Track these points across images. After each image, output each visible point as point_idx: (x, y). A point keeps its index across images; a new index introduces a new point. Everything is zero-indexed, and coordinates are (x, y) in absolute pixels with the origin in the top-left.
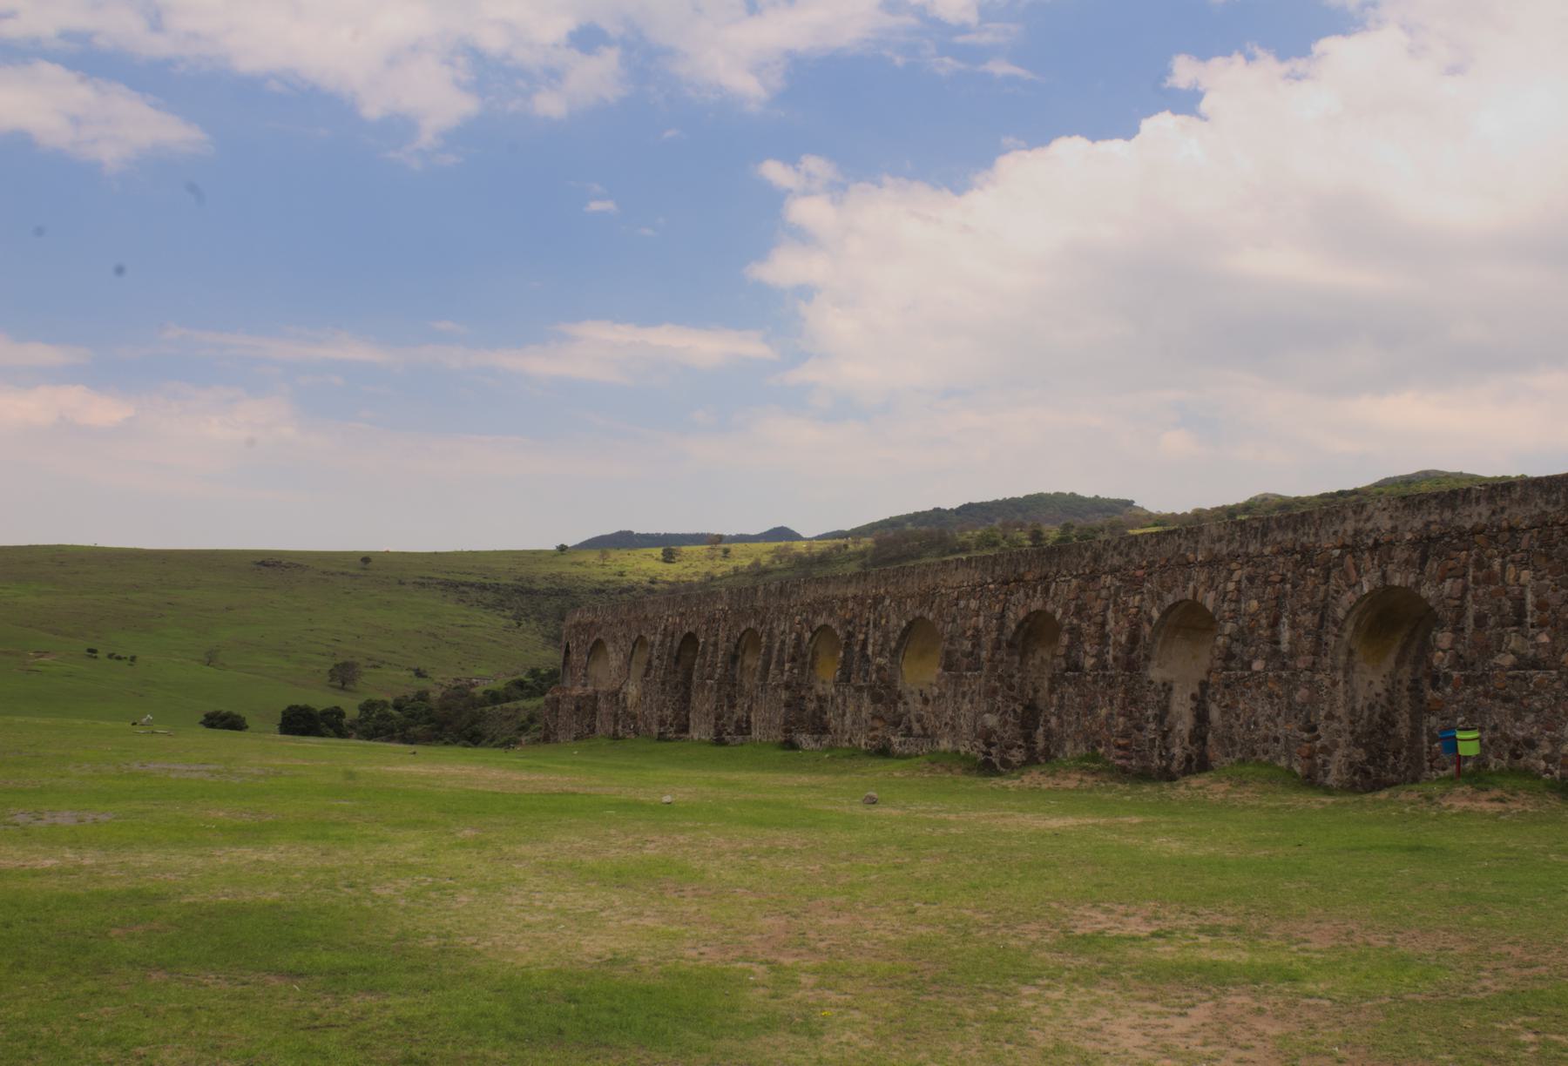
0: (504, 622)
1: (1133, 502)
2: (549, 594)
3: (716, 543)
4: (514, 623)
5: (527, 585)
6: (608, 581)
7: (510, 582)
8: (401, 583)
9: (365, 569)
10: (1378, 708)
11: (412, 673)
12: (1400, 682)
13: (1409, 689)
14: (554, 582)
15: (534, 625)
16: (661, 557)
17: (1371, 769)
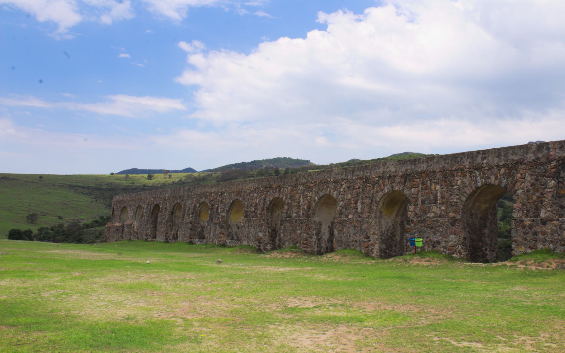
0: (91, 200)
1: (310, 161)
2: (107, 190)
3: (167, 173)
4: (94, 200)
5: (100, 187)
6: (128, 186)
8: (54, 186)
9: (41, 181)
10: (390, 231)
11: (58, 218)
12: (397, 222)
13: (400, 225)
14: (109, 186)
15: (102, 201)
16: (147, 178)
17: (387, 251)
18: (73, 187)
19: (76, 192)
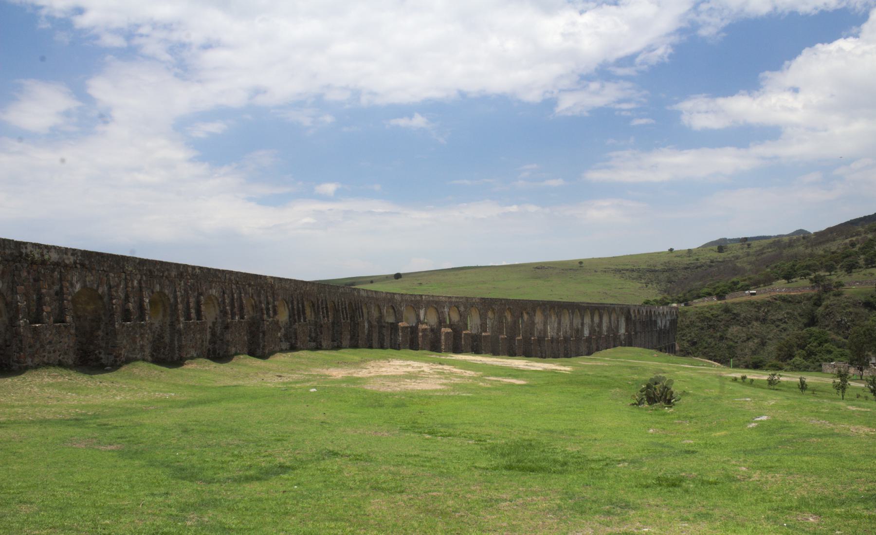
2: (664, 271)
3: (745, 241)
5: (653, 268)
6: (691, 263)
7: (644, 267)
8: (596, 271)
16: (717, 250)
18: (619, 271)
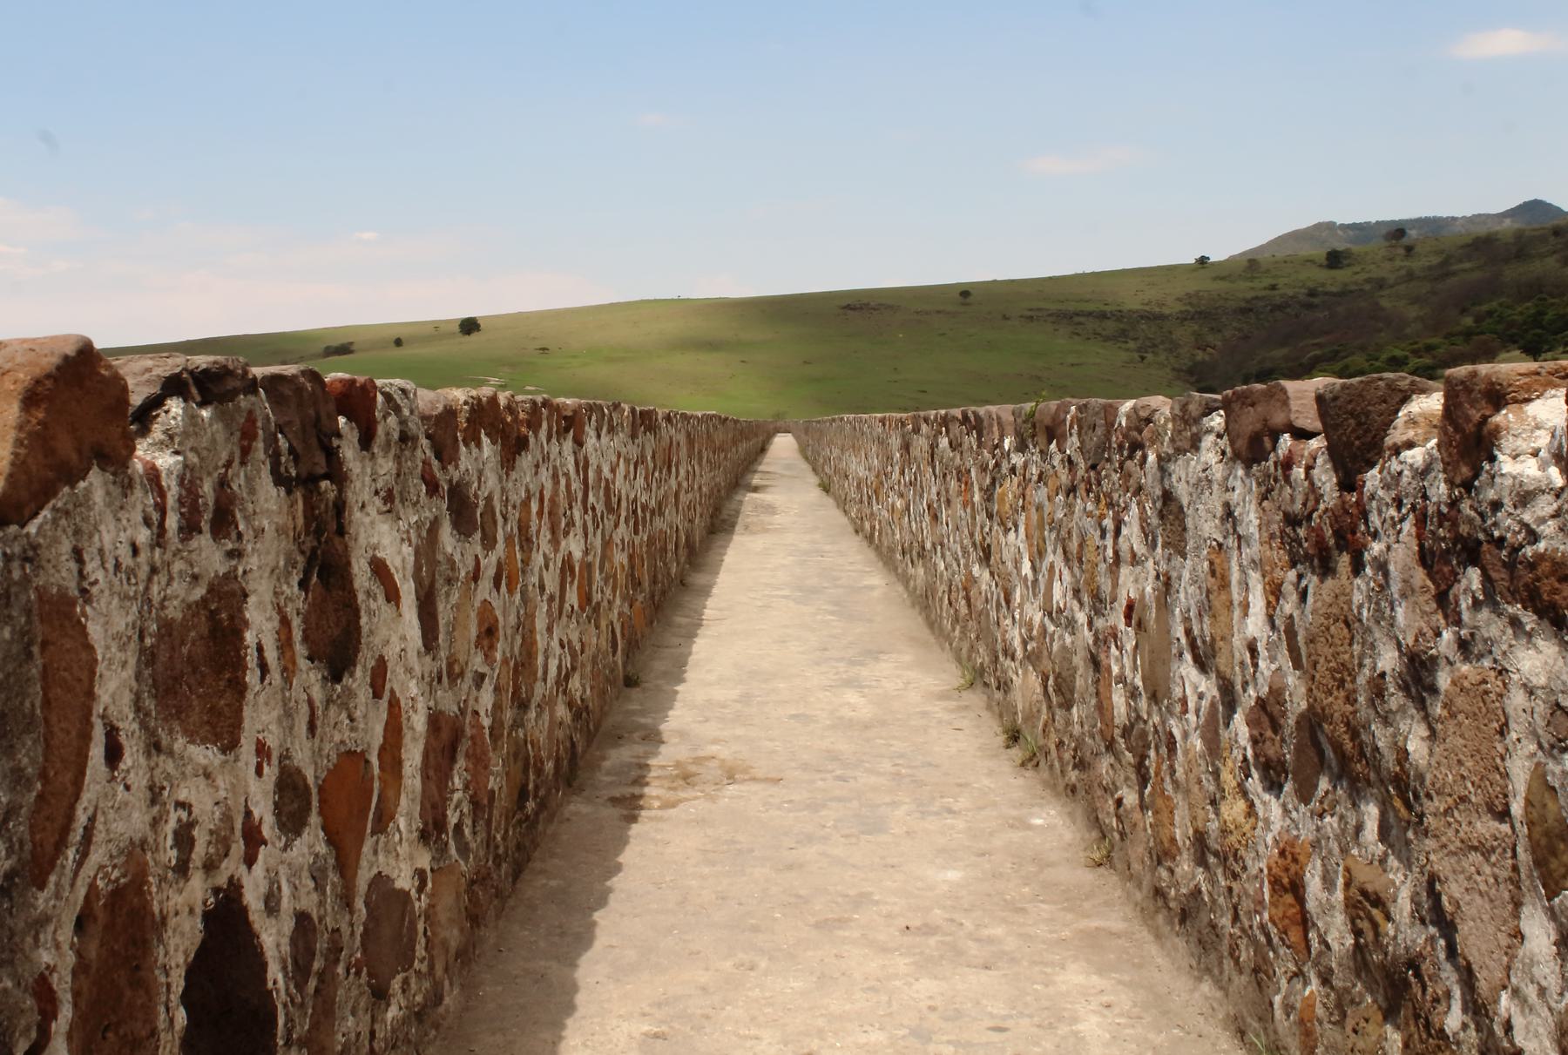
0: (1124, 356)
2: (1184, 318)
5: (1157, 310)
6: (1256, 298)
8: (1005, 318)
9: (963, 304)
14: (1190, 304)
15: (1162, 357)
16: (1325, 263)
19: (1078, 334)
